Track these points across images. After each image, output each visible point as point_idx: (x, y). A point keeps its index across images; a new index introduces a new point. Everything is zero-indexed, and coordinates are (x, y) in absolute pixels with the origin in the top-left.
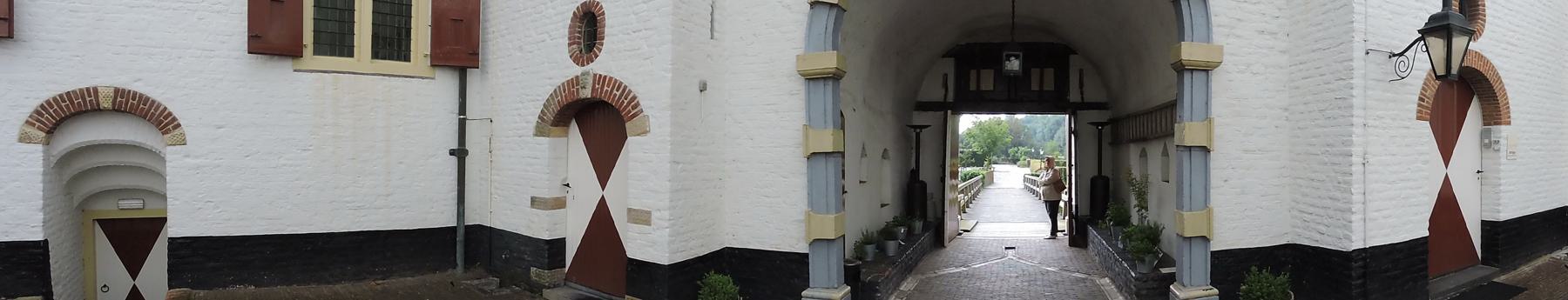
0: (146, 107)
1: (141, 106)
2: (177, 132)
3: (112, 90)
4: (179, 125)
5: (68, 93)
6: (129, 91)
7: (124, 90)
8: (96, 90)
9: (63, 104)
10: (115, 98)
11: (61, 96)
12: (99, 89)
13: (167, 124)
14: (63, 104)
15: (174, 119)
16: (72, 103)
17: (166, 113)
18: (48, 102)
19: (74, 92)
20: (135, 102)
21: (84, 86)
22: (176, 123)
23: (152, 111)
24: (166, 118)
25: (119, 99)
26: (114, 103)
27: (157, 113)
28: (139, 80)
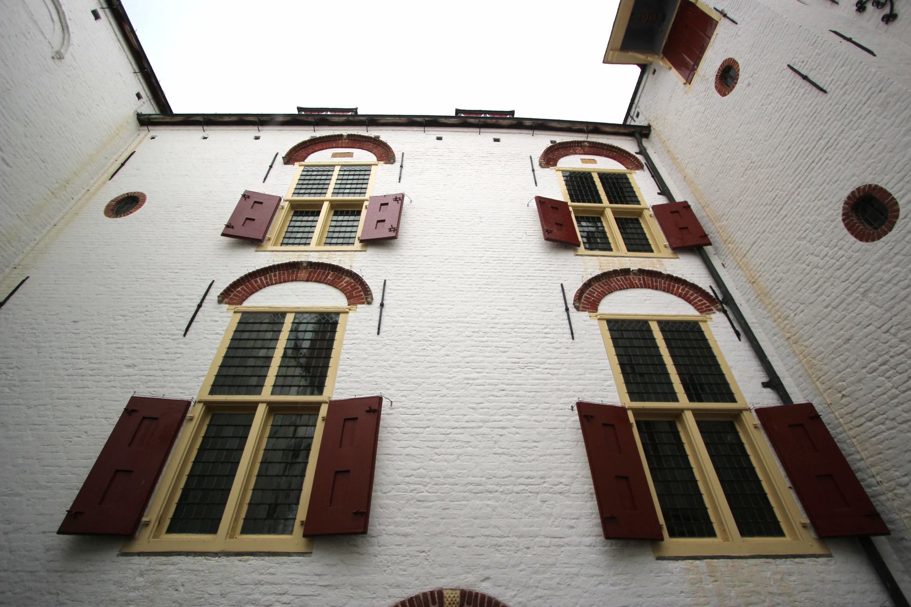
3: (458, 593)
6: (477, 594)
7: (470, 593)
8: (440, 593)
12: (445, 593)
19: (417, 597)
21: (427, 589)
28: (487, 579)
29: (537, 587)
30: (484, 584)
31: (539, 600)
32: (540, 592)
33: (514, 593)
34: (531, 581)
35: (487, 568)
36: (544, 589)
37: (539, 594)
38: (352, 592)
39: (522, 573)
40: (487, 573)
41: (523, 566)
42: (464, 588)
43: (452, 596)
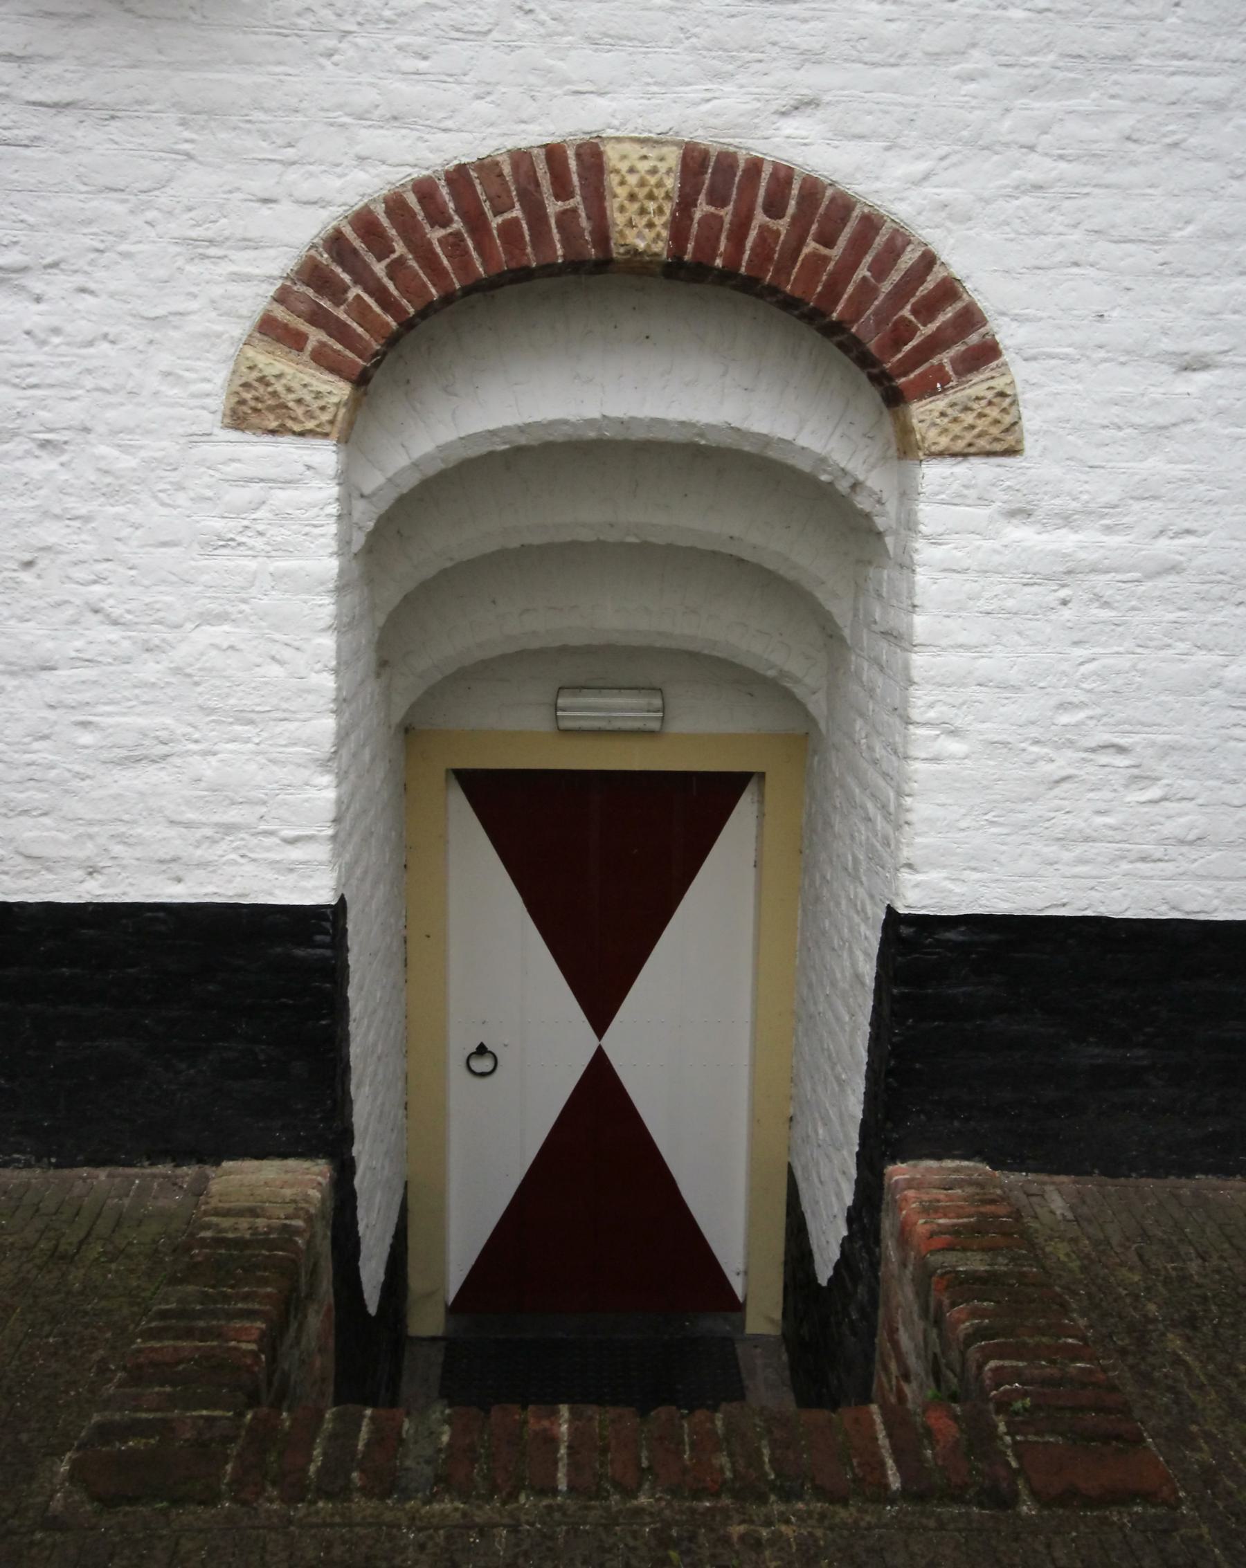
0: (836, 252)
1: (811, 246)
2: (978, 385)
3: (673, 157)
4: (988, 352)
5: (459, 177)
6: (755, 166)
7: (727, 161)
9: (435, 235)
10: (686, 204)
11: (425, 190)
12: (612, 154)
13: (934, 345)
14: (435, 235)
15: (971, 318)
16: (476, 223)
17: (930, 283)
18: (365, 222)
19: (488, 167)
20: (782, 225)
21: (533, 136)
22: (974, 339)
23: (863, 272)
24: (928, 309)
25: (702, 208)
26: (679, 228)
27: (886, 287)
29: (1032, 148)
30: (790, 126)
31: (1026, 200)
32: (1038, 168)
33: (922, 166)
34: (1007, 124)
35: (810, 58)
36: (1061, 157)
37: (1033, 177)
38: (187, 134)
39: (972, 87)
40: (808, 80)
41: (978, 60)
42: (703, 138)
43: (644, 166)
